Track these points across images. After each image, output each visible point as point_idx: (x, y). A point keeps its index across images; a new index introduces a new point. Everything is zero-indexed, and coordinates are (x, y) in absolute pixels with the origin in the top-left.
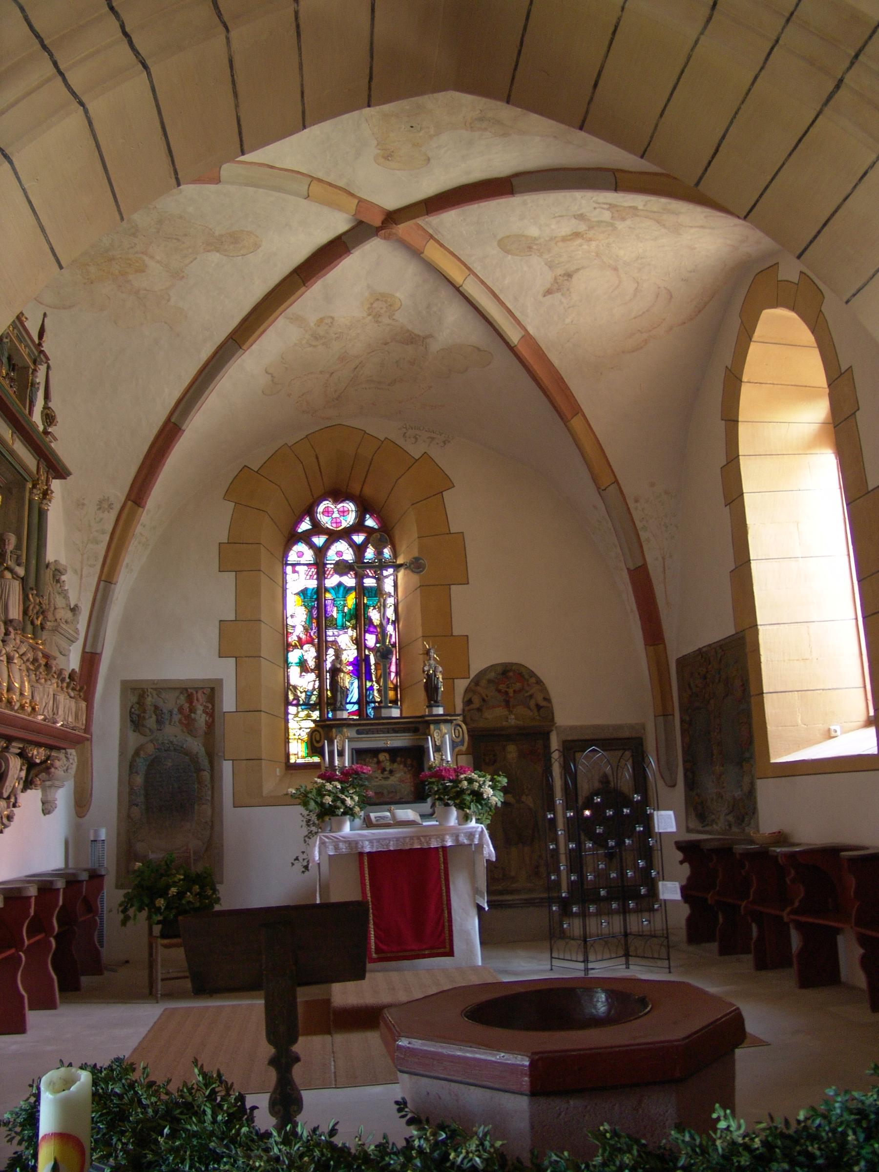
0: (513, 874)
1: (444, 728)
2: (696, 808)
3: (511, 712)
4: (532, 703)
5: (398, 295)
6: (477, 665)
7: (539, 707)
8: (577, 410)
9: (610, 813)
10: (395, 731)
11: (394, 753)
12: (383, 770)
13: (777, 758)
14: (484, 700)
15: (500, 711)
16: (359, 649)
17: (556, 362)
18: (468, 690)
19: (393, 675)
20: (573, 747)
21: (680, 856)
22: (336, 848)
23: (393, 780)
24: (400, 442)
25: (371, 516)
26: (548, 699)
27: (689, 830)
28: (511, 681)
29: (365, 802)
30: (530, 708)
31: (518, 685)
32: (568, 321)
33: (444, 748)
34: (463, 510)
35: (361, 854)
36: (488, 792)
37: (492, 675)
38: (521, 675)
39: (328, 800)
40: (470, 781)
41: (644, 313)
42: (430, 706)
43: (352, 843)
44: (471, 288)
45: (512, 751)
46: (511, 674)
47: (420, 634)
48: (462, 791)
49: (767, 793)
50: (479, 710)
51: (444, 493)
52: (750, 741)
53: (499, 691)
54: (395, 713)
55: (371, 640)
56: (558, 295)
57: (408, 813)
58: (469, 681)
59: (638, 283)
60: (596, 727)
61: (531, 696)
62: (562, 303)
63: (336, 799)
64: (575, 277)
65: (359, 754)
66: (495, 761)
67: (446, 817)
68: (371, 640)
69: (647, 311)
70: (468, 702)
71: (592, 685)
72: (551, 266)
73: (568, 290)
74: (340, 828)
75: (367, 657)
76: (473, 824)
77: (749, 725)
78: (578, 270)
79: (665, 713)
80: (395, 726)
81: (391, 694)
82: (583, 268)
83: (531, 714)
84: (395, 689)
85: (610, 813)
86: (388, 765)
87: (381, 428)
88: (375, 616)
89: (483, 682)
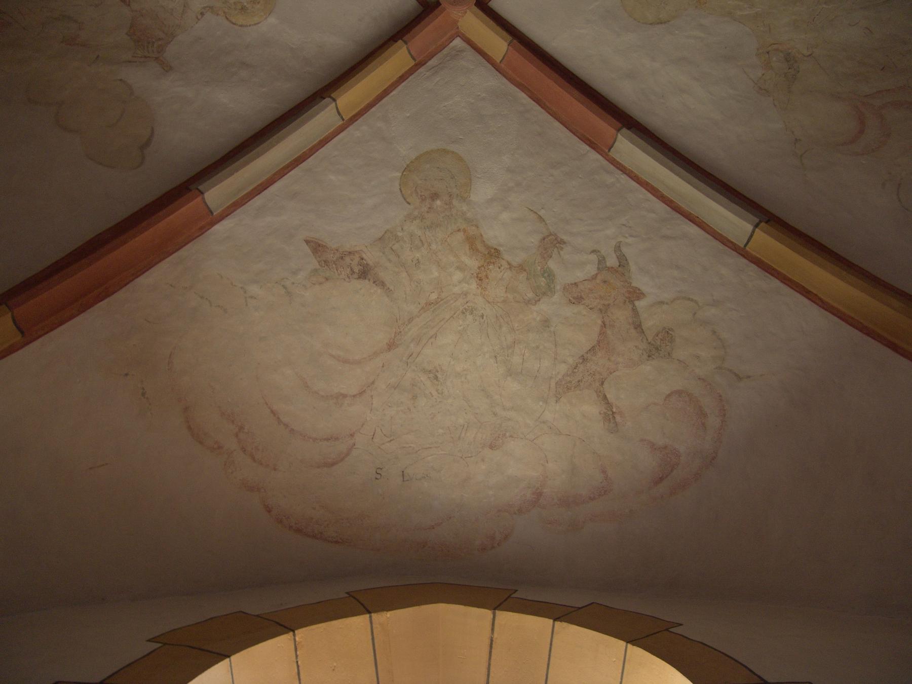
5: (272, 20)
17: (145, 280)
32: (254, 289)
41: (286, 426)
44: (323, 118)
56: (313, 263)
59: (361, 393)
62: (295, 273)
64: (365, 284)
69: (292, 431)
72: (385, 240)
73: (327, 279)
78: (382, 284)
82: (388, 292)
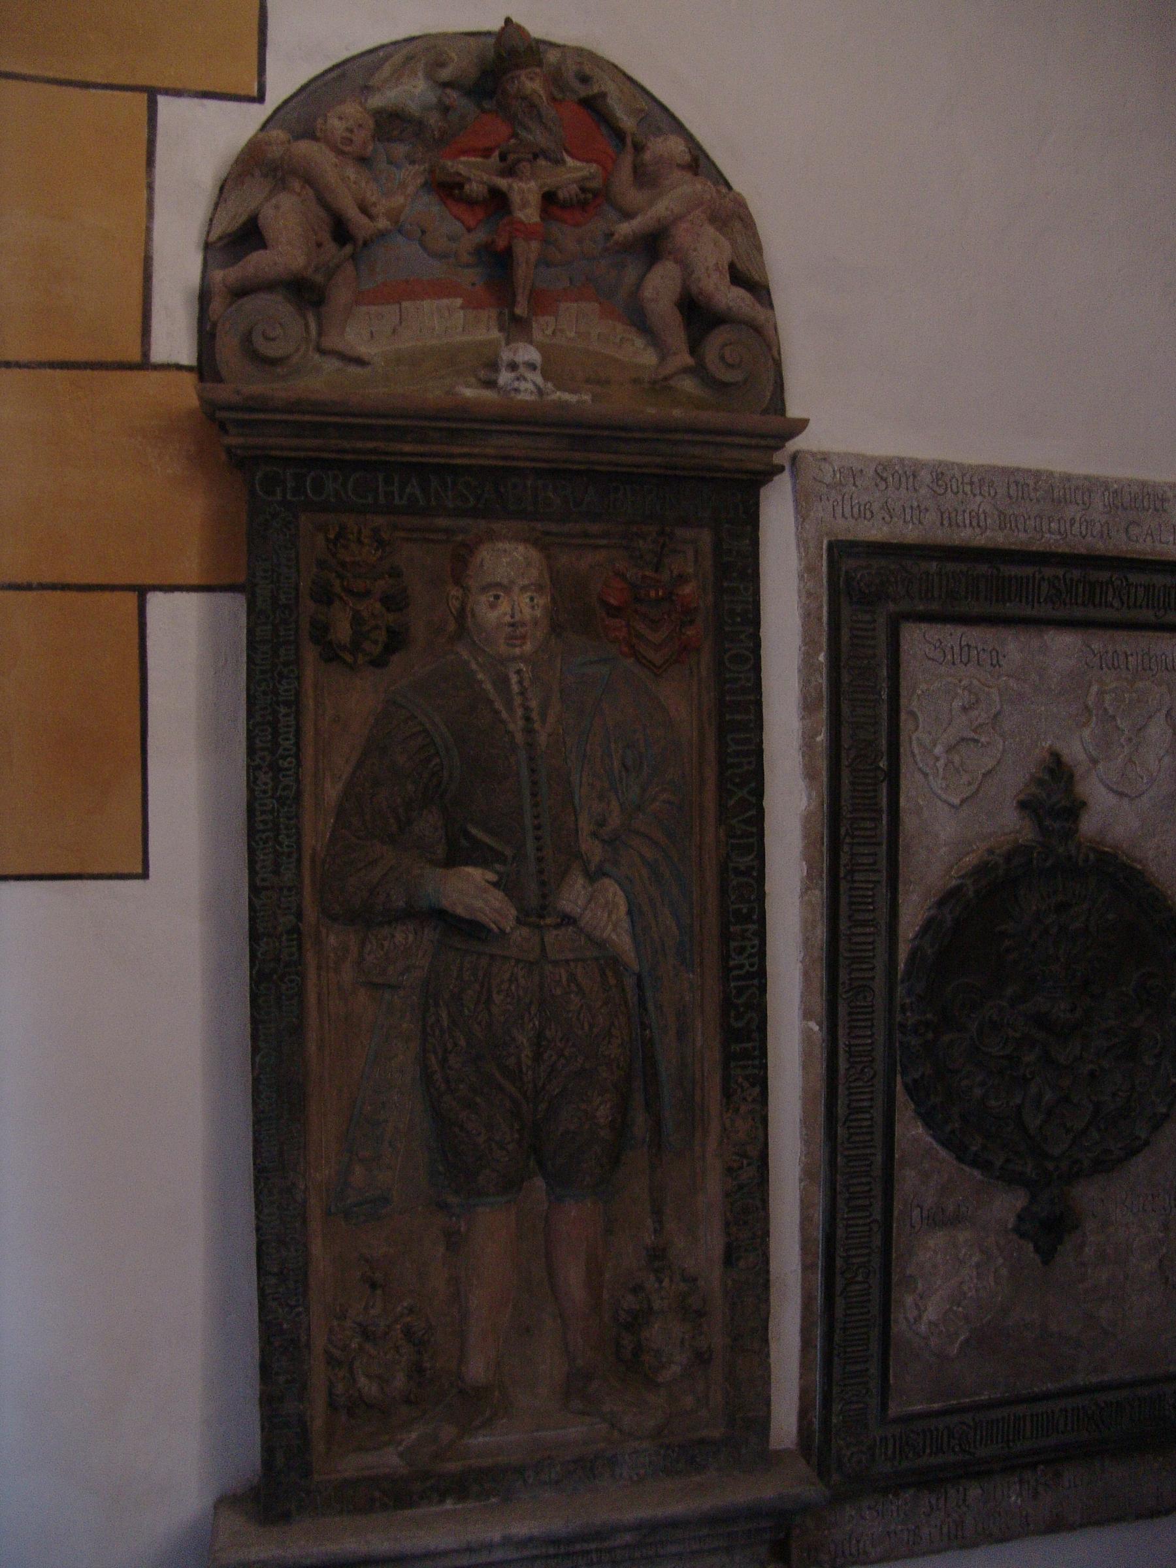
0: (477, 1369)
3: (516, 327)
4: (661, 286)
7: (698, 315)
14: (341, 232)
15: (446, 323)
30: (639, 319)
38: (594, 106)
45: (509, 584)
46: (532, 84)
50: (306, 292)
53: (447, 189)
58: (259, 113)
60: (1022, 483)
61: (653, 246)
66: (396, 640)
70: (235, 240)
83: (649, 358)
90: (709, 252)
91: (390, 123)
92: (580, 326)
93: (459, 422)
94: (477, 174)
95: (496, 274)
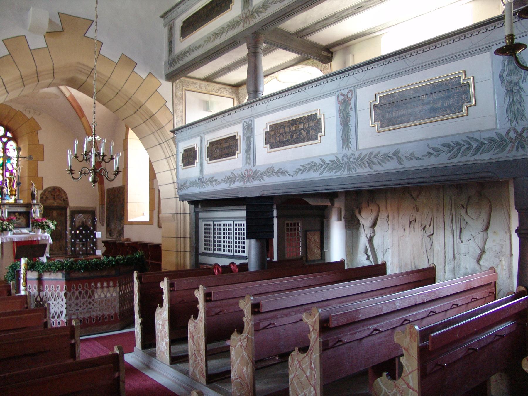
1: (37, 207)
2: (109, 232)
4: (62, 199)
6: (45, 187)
7: (64, 200)
8: (84, 115)
9: (84, 232)
10: (21, 207)
11: (20, 213)
12: (17, 218)
13: (129, 220)
15: (52, 201)
16: (3, 177)
18: (42, 194)
19: (15, 187)
20: (74, 213)
21: (103, 244)
22: (6, 240)
23: (20, 221)
24: (24, 112)
25: (10, 132)
26: (67, 198)
27: (107, 238)
28: (56, 192)
29: (15, 227)
31: (58, 193)
33: (37, 212)
34: (45, 137)
35: (14, 242)
36: (51, 225)
37: (50, 190)
38: (59, 190)
39: (5, 227)
40: (46, 223)
42: (32, 200)
43: (10, 238)
45: (55, 213)
47: (27, 175)
48: (44, 225)
49: (126, 228)
50: (45, 200)
51: (38, 132)
52: (124, 215)
54: (21, 202)
55: (8, 174)
57: (25, 231)
63: (7, 226)
65: (9, 213)
67: (38, 232)
68: (8, 174)
71: (81, 195)
74: (7, 234)
75: (6, 180)
76: (46, 234)
77: (124, 211)
79: (102, 204)
80: (22, 206)
81: (14, 193)
84: (16, 191)
85: (84, 232)
86: (18, 217)
87: (18, 107)
88: (9, 166)
89: (47, 192)
90: (65, 197)
91: (49, 192)
92: (58, 201)
93: (52, 206)
94: (53, 194)
95: (54, 199)
